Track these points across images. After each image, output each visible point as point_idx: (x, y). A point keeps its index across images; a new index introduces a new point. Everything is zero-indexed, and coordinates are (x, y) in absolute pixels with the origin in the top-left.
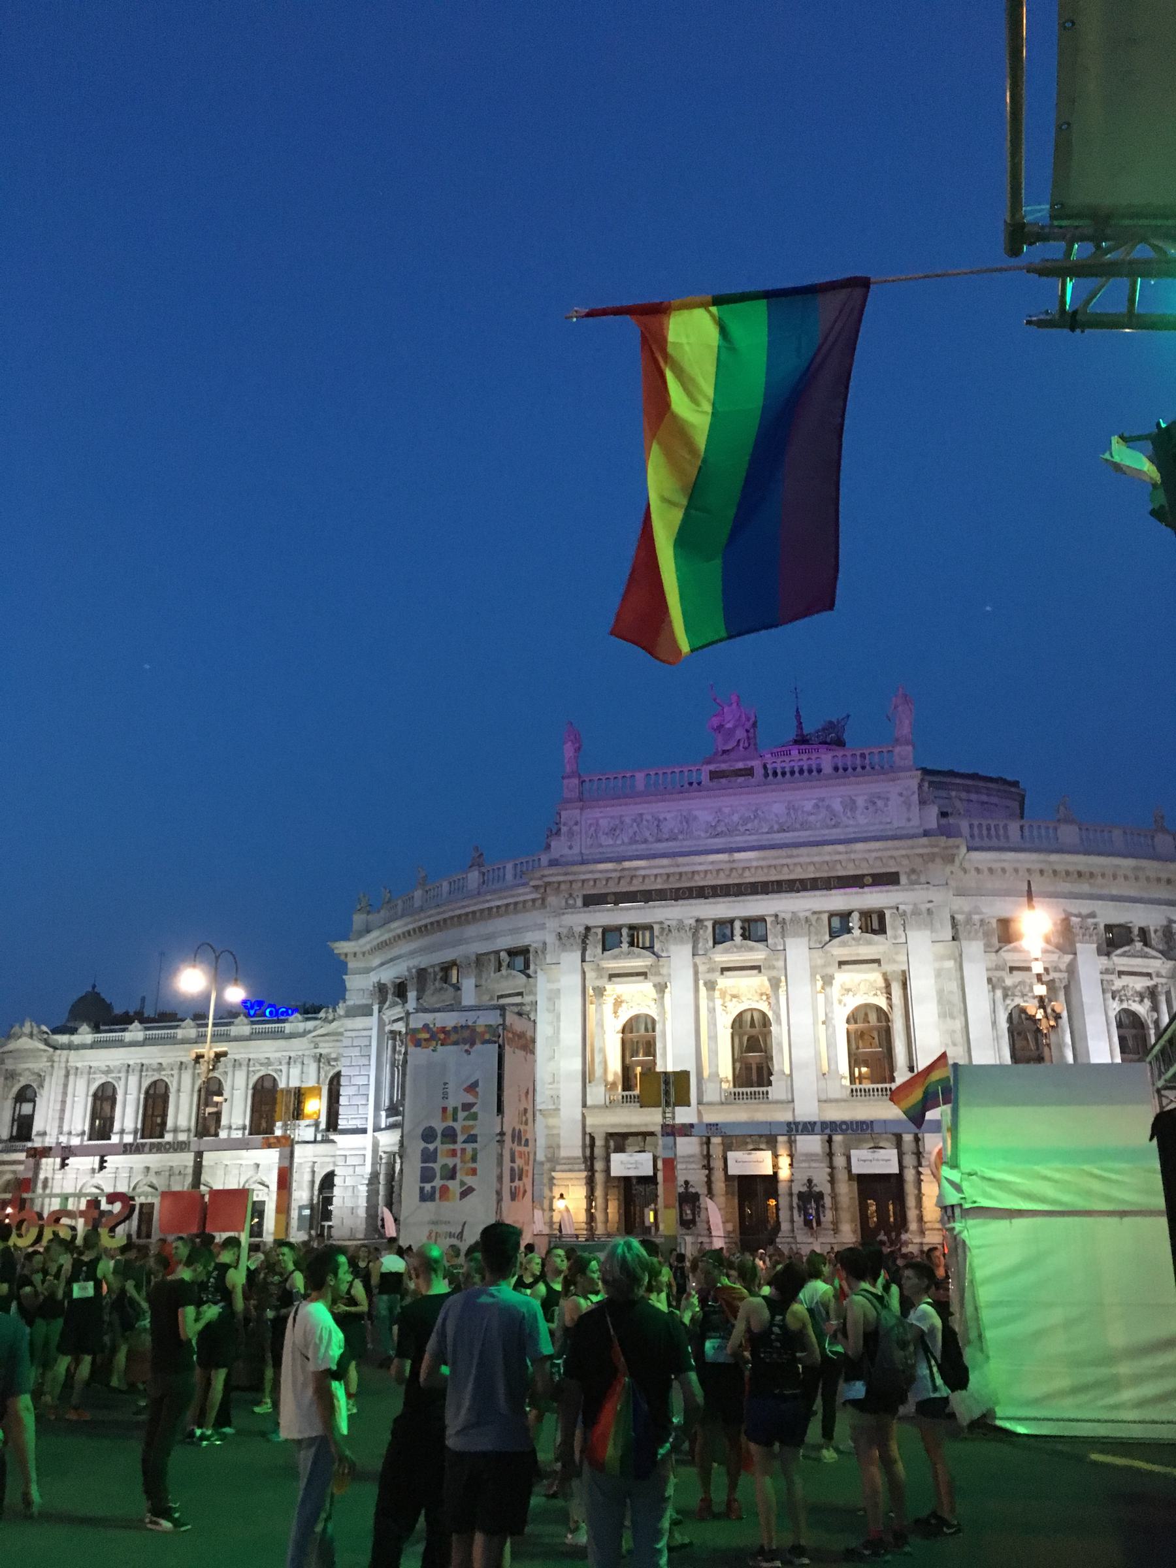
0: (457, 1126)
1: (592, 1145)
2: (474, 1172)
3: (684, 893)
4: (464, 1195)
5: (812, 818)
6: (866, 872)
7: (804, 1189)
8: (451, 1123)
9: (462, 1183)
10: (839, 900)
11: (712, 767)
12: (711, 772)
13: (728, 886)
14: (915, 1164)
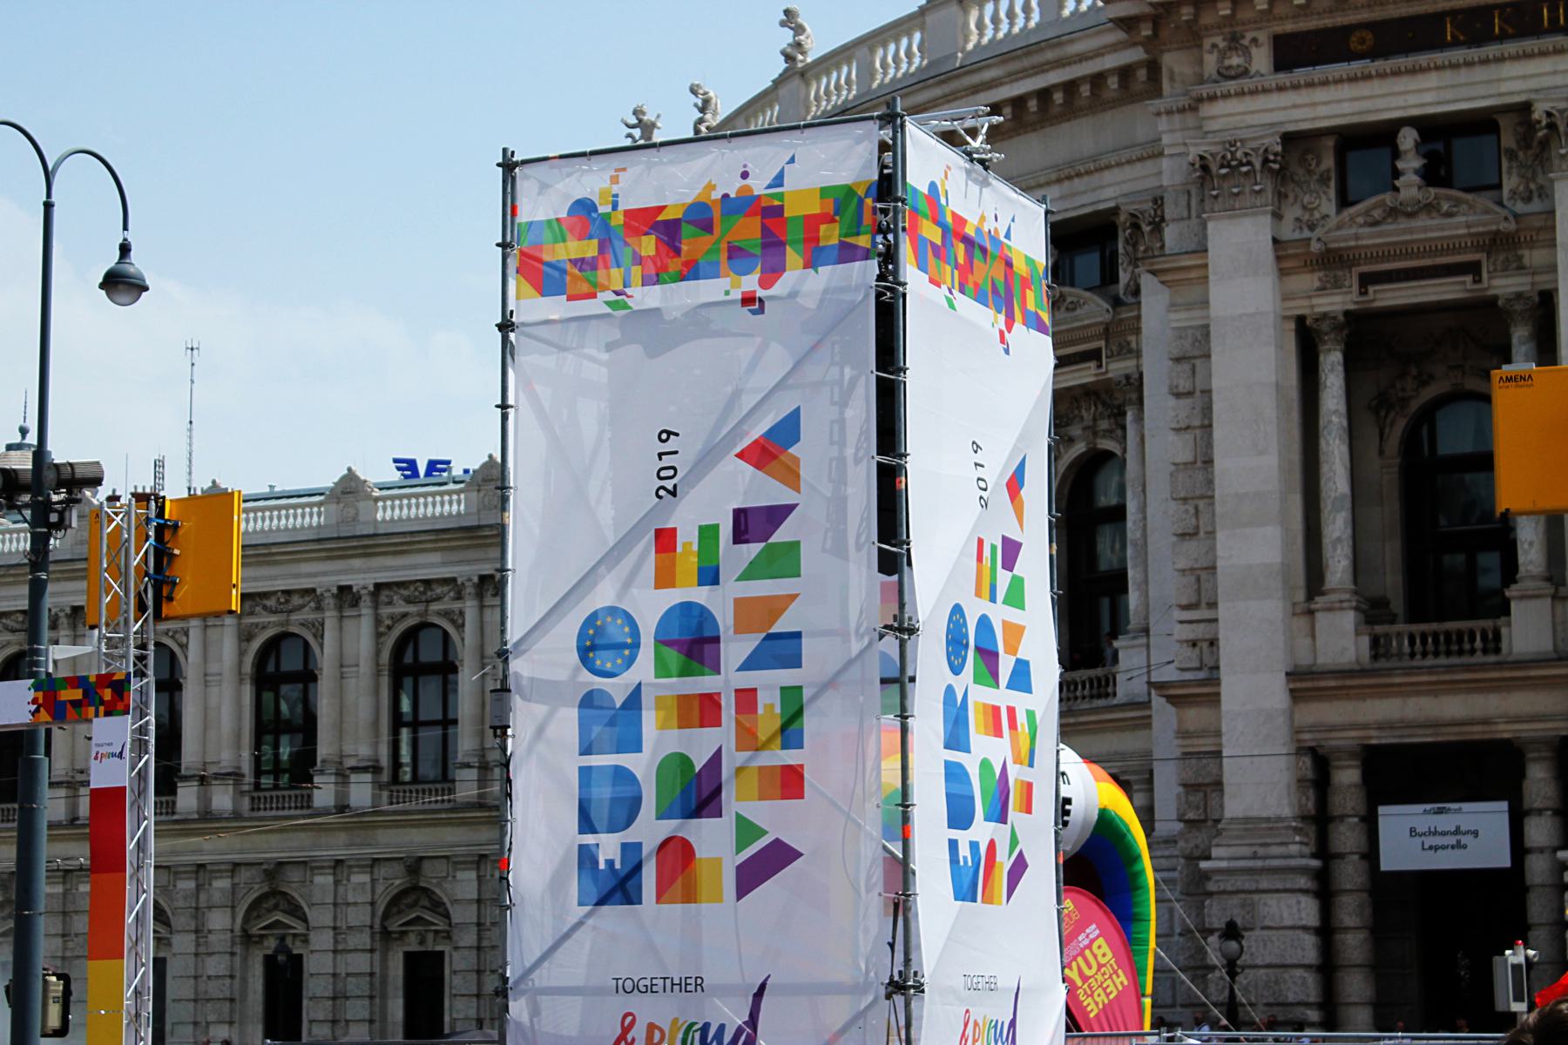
0: (719, 602)
2: (790, 782)
4: (751, 876)
8: (700, 595)
9: (746, 830)
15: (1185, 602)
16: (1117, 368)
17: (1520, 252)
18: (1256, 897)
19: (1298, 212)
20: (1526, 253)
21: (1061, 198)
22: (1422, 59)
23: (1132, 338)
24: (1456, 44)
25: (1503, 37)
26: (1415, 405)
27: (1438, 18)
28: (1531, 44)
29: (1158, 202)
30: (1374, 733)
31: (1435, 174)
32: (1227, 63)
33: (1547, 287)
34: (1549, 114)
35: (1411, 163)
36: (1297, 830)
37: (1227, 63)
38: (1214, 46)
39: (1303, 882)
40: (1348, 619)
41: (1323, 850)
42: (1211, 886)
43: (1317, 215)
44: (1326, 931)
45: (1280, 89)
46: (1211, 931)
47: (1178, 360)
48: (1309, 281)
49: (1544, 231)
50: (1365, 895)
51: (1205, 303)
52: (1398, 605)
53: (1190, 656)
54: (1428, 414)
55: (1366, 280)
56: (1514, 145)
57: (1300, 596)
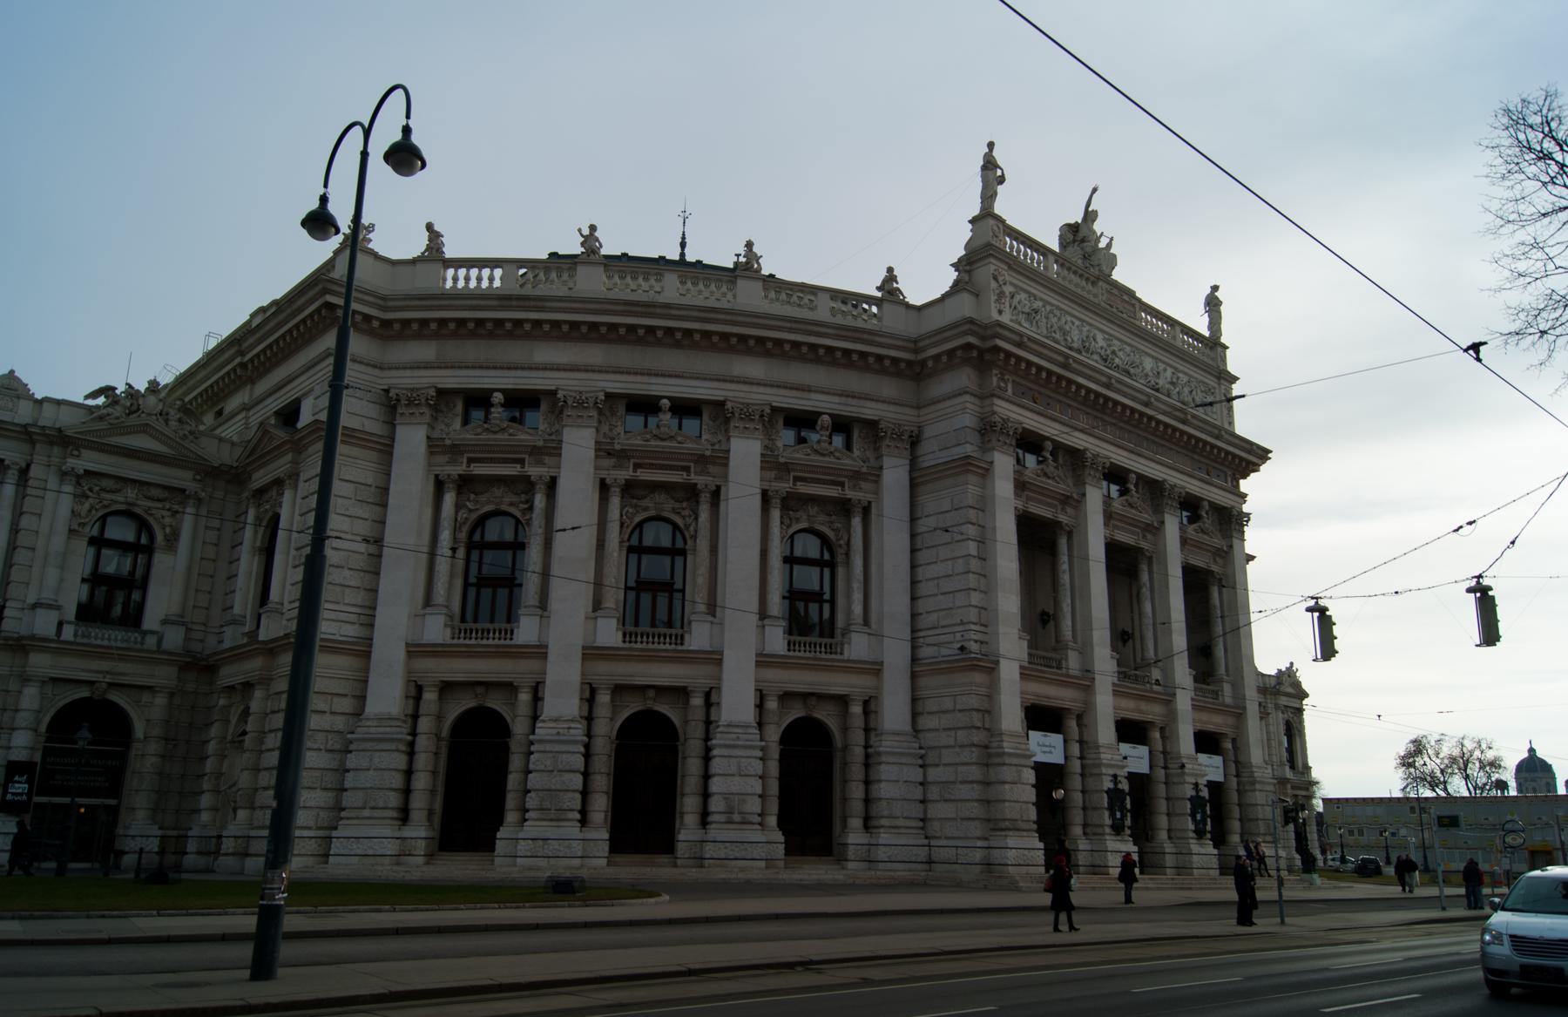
1: (418, 698)
40: (441, 619)
42: (352, 747)
44: (409, 773)
48: (442, 459)
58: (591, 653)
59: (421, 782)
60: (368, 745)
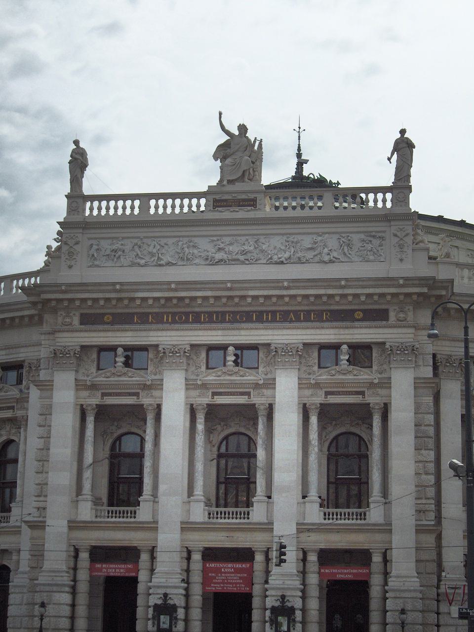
3: (180, 318)
5: (309, 255)
6: (356, 307)
7: (277, 604)
10: (327, 334)
11: (217, 197)
12: (215, 201)
13: (224, 313)
14: (382, 583)
15: (36, 495)
16: (19, 413)
17: (152, 391)
18: (53, 593)
19: (84, 371)
20: (153, 391)
21: (5, 355)
22: (127, 327)
23: (26, 404)
24: (137, 323)
25: (152, 323)
26: (115, 435)
27: (133, 314)
28: (160, 326)
29: (39, 360)
30: (93, 542)
31: (127, 363)
32: (65, 320)
33: (159, 403)
34: (164, 349)
35: (121, 359)
36: (67, 572)
37: (65, 320)
38: (61, 314)
39: (67, 589)
40: (89, 504)
41: (75, 580)
43: (90, 372)
44: (73, 606)
45: (81, 331)
46: (36, 604)
47: (41, 415)
48: (85, 393)
49: (158, 386)
50: (87, 594)
51: (51, 397)
52: (105, 500)
53: (36, 514)
54: (119, 438)
55: (103, 395)
56: (153, 357)
57: (74, 494)
58: (187, 527)
59: (82, 611)
60: (47, 588)
